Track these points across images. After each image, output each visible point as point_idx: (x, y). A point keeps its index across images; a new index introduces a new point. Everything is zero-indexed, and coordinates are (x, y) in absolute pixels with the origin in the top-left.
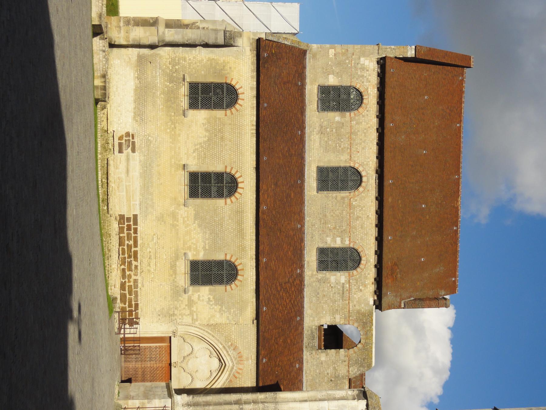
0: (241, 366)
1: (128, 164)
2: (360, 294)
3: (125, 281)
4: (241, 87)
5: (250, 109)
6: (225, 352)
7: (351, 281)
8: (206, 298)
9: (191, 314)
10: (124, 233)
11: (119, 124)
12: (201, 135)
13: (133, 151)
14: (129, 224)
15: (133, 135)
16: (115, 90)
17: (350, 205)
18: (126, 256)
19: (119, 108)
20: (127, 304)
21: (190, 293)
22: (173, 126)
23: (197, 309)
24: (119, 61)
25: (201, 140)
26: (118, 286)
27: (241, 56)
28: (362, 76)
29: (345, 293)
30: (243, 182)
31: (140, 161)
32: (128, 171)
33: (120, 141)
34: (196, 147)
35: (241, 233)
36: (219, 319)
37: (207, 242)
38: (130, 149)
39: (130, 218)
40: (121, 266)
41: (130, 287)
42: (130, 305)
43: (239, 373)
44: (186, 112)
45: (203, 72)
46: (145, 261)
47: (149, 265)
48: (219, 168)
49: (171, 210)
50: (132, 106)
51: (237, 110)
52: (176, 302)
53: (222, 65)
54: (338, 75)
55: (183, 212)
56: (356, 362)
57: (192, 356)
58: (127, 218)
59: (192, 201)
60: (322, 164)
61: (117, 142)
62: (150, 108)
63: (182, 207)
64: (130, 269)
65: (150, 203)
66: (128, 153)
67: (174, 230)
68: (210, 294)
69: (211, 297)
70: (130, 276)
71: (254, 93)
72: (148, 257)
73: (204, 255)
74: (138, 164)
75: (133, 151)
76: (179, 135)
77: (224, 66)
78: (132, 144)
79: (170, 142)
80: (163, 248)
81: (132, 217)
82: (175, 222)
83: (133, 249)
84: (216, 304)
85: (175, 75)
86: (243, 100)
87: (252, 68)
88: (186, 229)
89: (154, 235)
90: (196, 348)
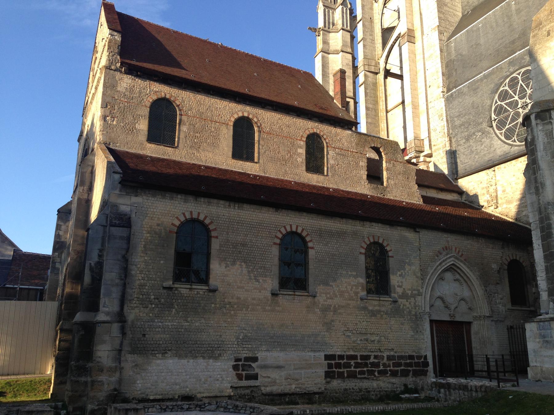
0: (454, 249)
1: (271, 367)
2: (344, 140)
3: (390, 370)
4: (184, 214)
5: (211, 207)
6: (443, 264)
7: (333, 146)
8: (400, 279)
9: (414, 296)
10: (344, 372)
11: (223, 380)
12: (239, 271)
13: (255, 359)
14: (336, 366)
15: (238, 360)
16: (178, 387)
17: (269, 133)
18: (365, 369)
19: (203, 380)
20: (409, 368)
21: (396, 296)
22: (228, 306)
23: (409, 290)
24: (138, 382)
25: (245, 271)
26: (393, 380)
27: (143, 209)
28: (140, 93)
29: (343, 152)
30: (291, 226)
31: (267, 350)
32: (279, 367)
33: (244, 379)
34: (253, 278)
35: (341, 234)
36: (416, 268)
37: (349, 273)
38: (253, 365)
39: (328, 364)
40: (375, 376)
41: (395, 365)
42: (410, 365)
43: (459, 251)
44: (212, 288)
45: (162, 262)
46: (370, 346)
47: (374, 341)
48: (275, 251)
49: (319, 312)
50: (200, 361)
51: (212, 223)
52: (405, 312)
53: (154, 236)
54: (136, 118)
55: (321, 299)
56: (394, 154)
57: (445, 298)
58: (328, 368)
59: (311, 288)
60: (230, 154)
61: (244, 383)
62: (204, 336)
63: (316, 299)
64: (377, 365)
65: (313, 338)
66: (258, 367)
67: (339, 311)
68: (396, 274)
69: (399, 273)
70: (384, 365)
71: (191, 198)
72: (366, 342)
73: (361, 277)
74: (271, 353)
75: (255, 359)
76: (238, 298)
77: (156, 233)
78: (248, 361)
79: (247, 310)
80: (356, 324)
81: (326, 362)
82: (332, 308)
83: (359, 361)
84: (404, 269)
85: (163, 300)
86: (199, 214)
87: (160, 197)
88: (338, 296)
89: (344, 335)
90: (439, 294)
